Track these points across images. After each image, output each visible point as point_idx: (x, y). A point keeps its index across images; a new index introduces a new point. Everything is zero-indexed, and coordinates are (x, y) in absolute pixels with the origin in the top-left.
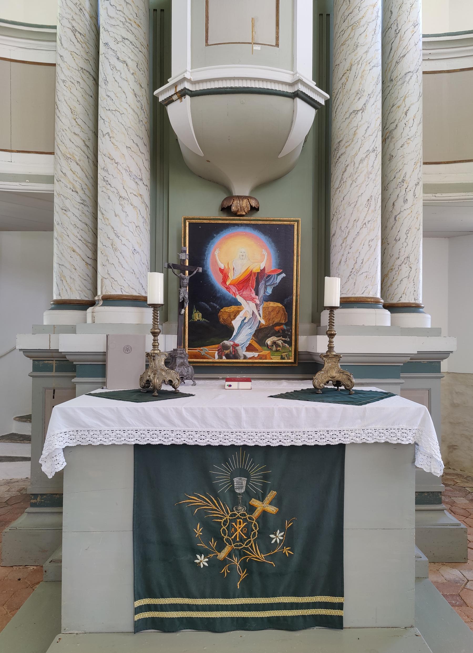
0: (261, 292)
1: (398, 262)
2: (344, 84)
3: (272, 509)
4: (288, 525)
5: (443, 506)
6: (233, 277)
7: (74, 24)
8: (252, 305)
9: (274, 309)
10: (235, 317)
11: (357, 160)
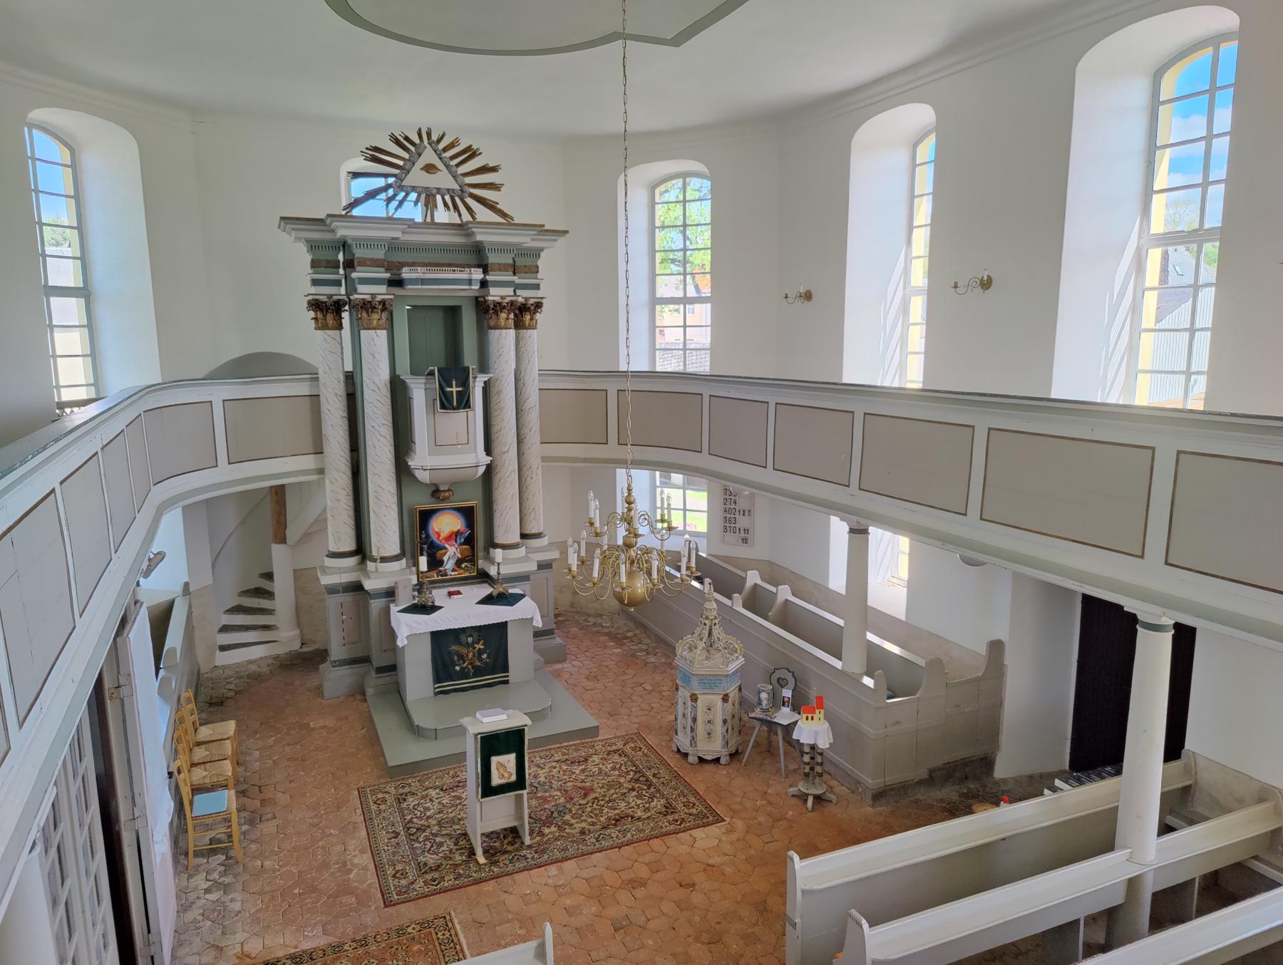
0: (458, 541)
1: (529, 511)
2: (498, 437)
3: (482, 647)
4: (488, 651)
5: (555, 635)
6: (443, 535)
7: (336, 391)
8: (454, 548)
9: (465, 549)
10: (444, 555)
11: (506, 476)
